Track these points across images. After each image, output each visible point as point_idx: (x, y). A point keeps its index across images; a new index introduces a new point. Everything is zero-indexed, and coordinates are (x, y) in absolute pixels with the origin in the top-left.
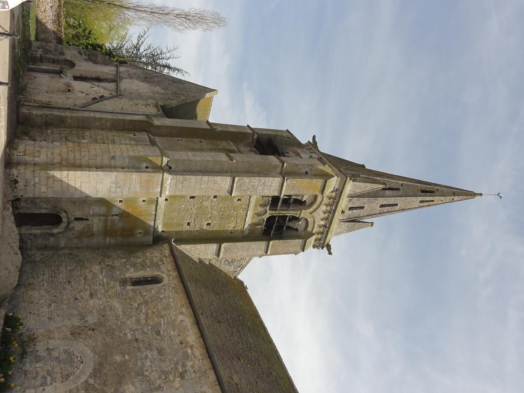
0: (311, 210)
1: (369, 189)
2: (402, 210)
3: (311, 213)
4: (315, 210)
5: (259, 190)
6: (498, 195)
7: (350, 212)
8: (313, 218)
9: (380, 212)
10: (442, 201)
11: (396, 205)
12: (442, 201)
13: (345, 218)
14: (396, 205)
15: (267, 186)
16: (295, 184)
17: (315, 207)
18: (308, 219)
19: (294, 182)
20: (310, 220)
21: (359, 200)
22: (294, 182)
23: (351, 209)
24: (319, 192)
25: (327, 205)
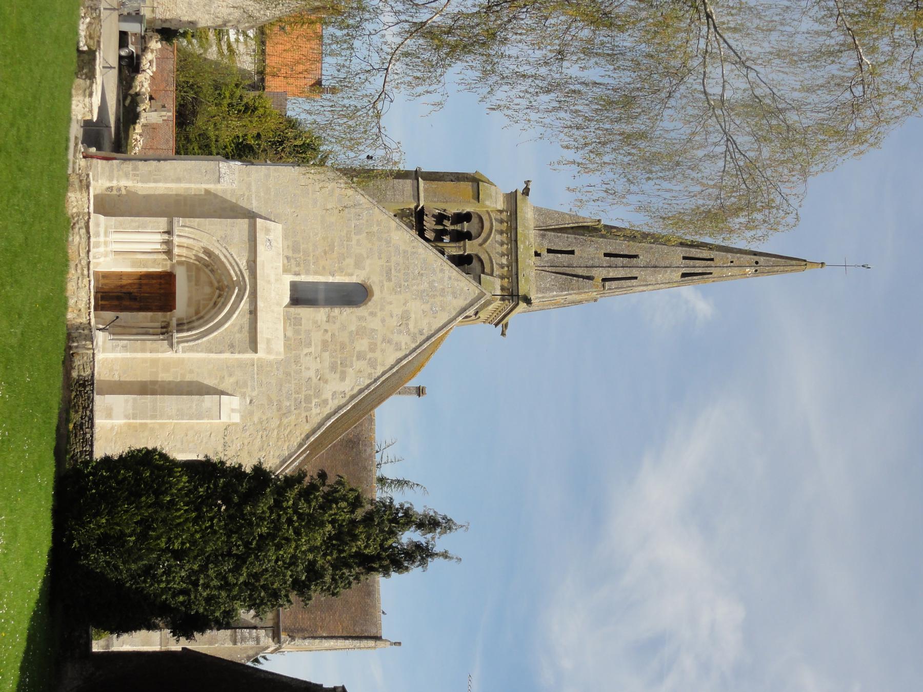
0: (480, 240)
1: (570, 222)
2: (653, 267)
3: (481, 245)
4: (485, 240)
5: (389, 195)
6: (863, 266)
7: (551, 255)
8: (487, 252)
9: (608, 265)
10: (732, 262)
11: (636, 256)
12: (732, 262)
13: (547, 265)
14: (636, 256)
15: (398, 190)
16: (435, 188)
17: (483, 235)
18: (480, 255)
19: (434, 186)
20: (484, 257)
21: (558, 237)
22: (434, 186)
23: (549, 251)
24: (473, 198)
25: (501, 233)
